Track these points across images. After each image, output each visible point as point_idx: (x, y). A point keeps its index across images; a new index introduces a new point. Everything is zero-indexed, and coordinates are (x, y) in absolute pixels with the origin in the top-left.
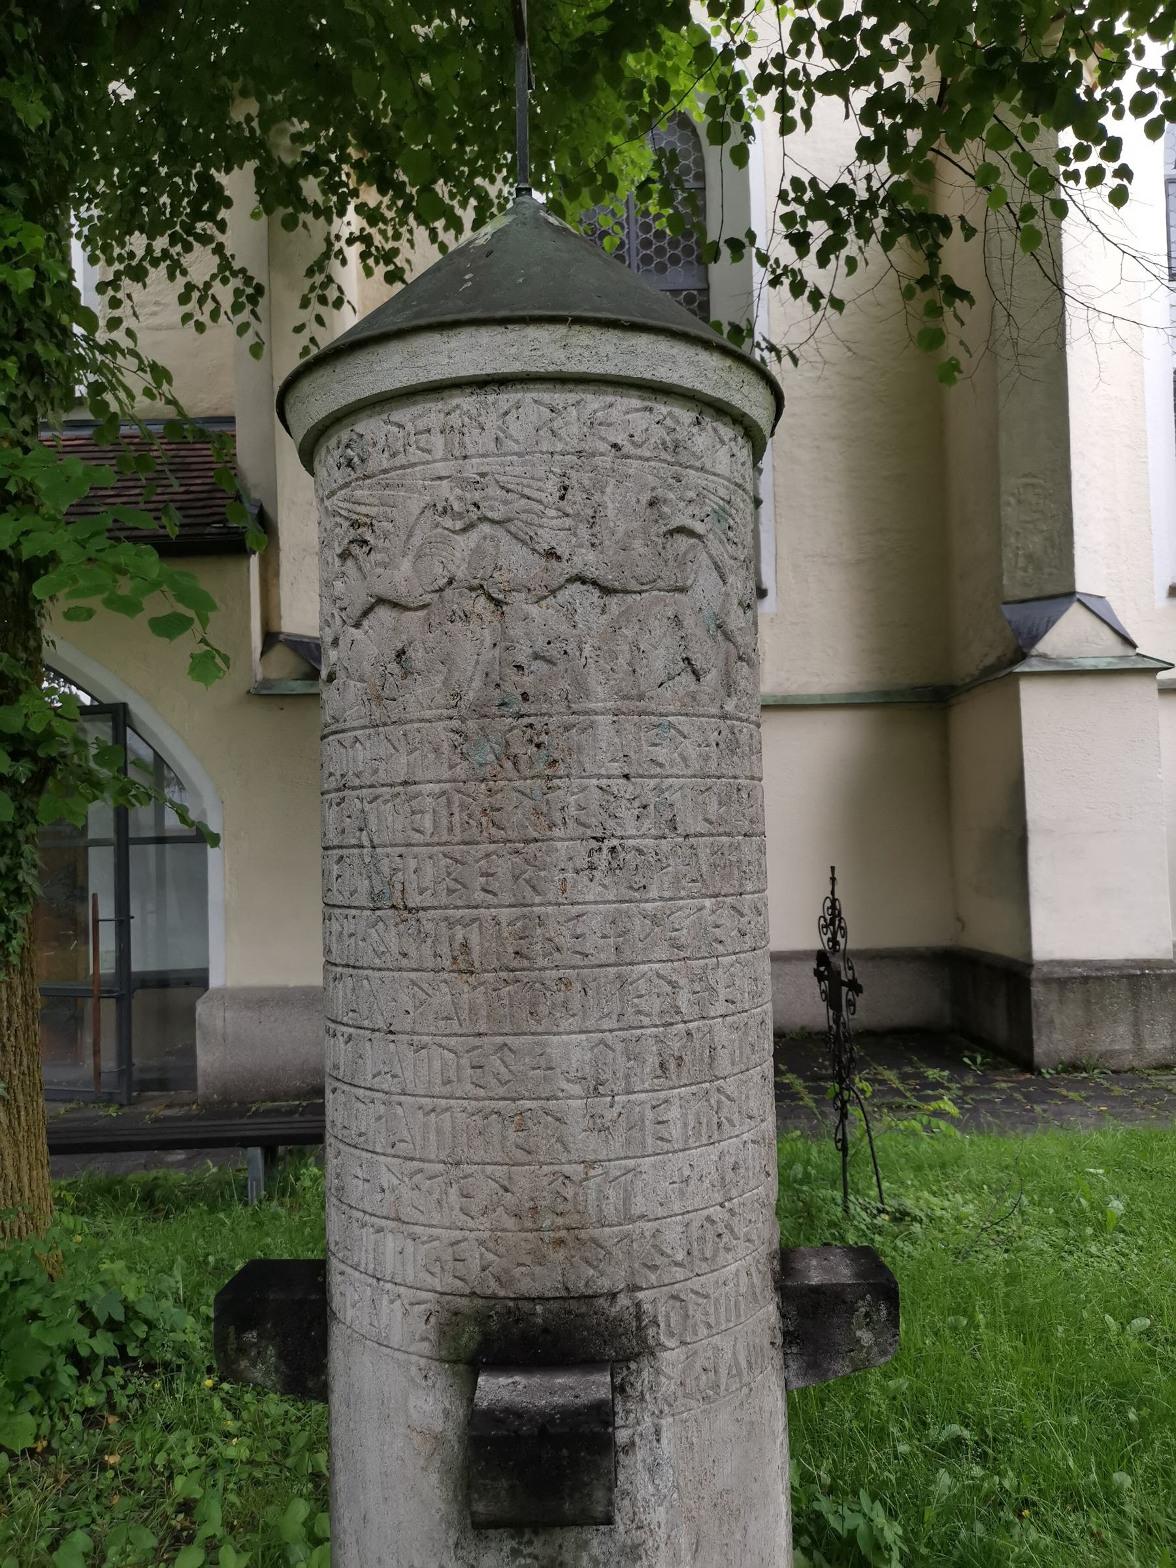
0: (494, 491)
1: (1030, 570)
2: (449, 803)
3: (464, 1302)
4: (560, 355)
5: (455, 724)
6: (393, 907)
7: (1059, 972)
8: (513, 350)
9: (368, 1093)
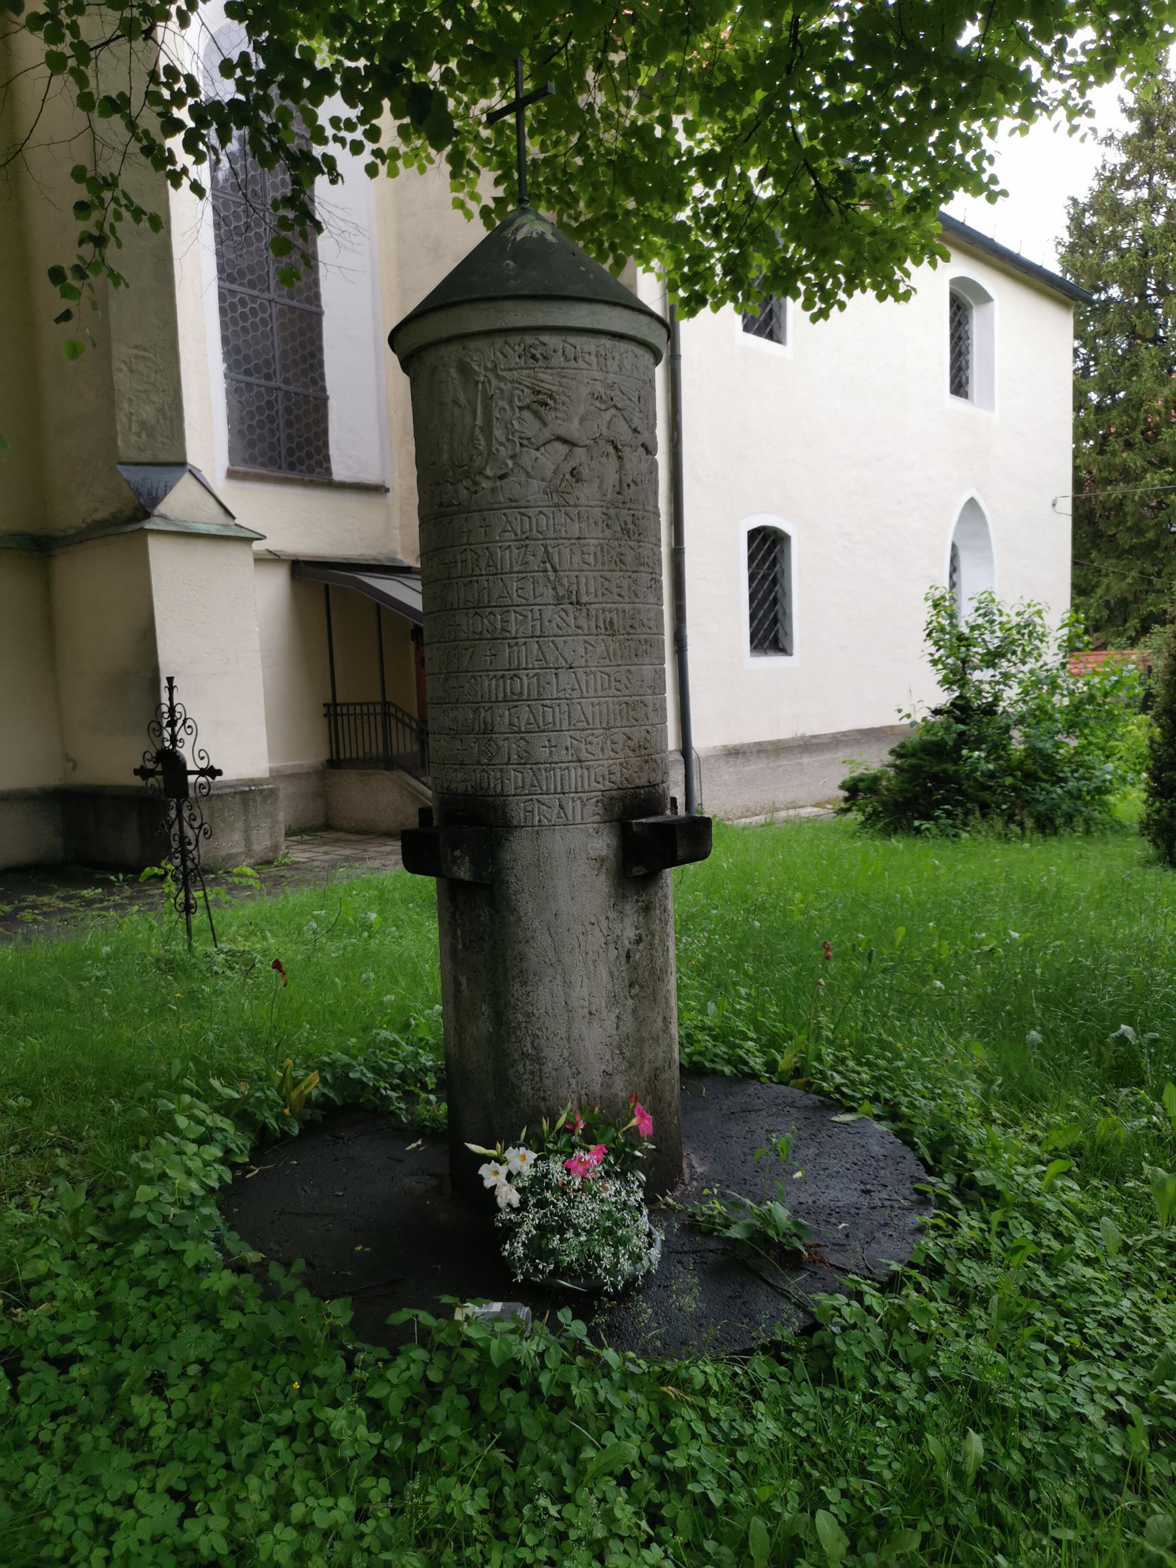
0: (617, 392)
1: (144, 435)
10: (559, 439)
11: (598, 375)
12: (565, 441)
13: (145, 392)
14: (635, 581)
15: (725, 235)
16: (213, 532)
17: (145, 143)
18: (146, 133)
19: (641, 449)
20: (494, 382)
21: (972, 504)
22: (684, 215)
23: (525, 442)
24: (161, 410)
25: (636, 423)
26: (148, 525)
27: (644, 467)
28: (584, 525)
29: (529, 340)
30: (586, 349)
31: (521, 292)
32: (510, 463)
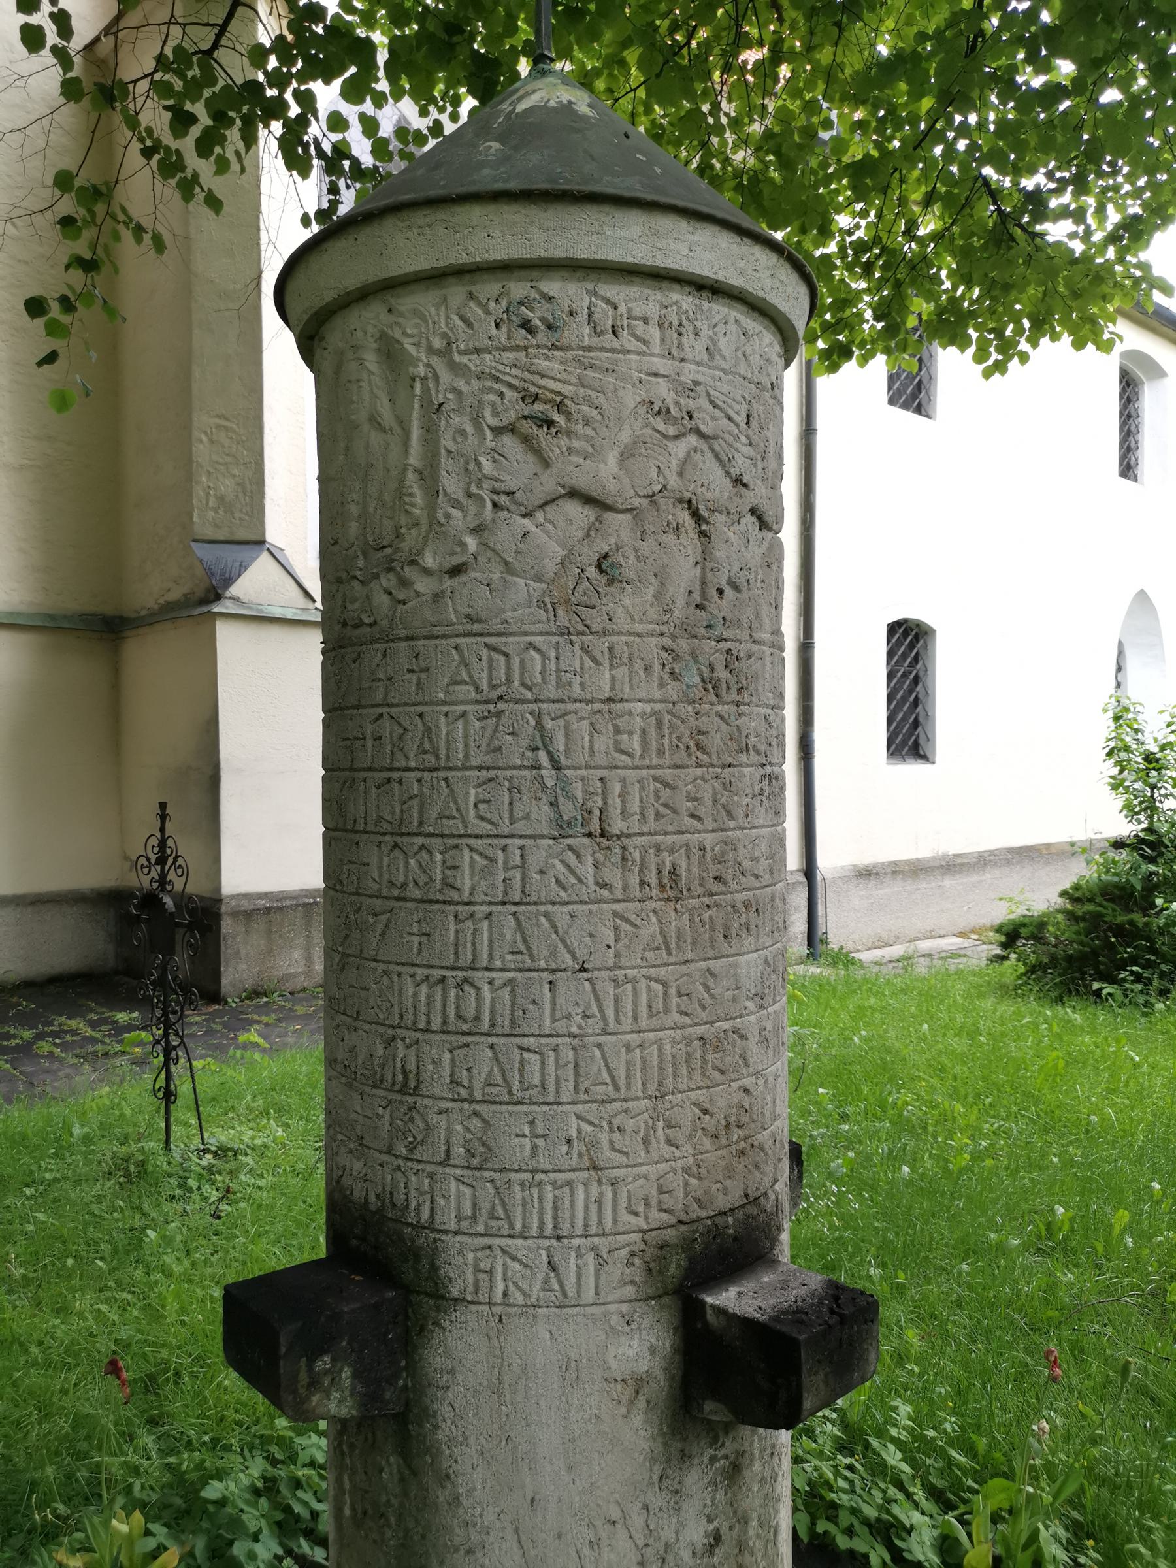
0: (703, 402)
1: (221, 512)
2: (659, 724)
3: (670, 1233)
4: (768, 283)
5: (666, 641)
6: (589, 835)
7: (246, 905)
8: (742, 264)
9: (549, 1040)
10: (573, 494)
11: (663, 365)
12: (588, 500)
13: (226, 464)
14: (728, 786)
15: (877, 275)
16: (289, 616)
17: (149, 143)
18: (149, 131)
19: (750, 520)
20: (445, 377)
22: (832, 248)
23: (503, 500)
24: (241, 484)
25: (741, 465)
26: (217, 608)
27: (754, 555)
28: (622, 672)
29: (518, 289)
30: (638, 309)
31: (499, 186)
32: (472, 543)
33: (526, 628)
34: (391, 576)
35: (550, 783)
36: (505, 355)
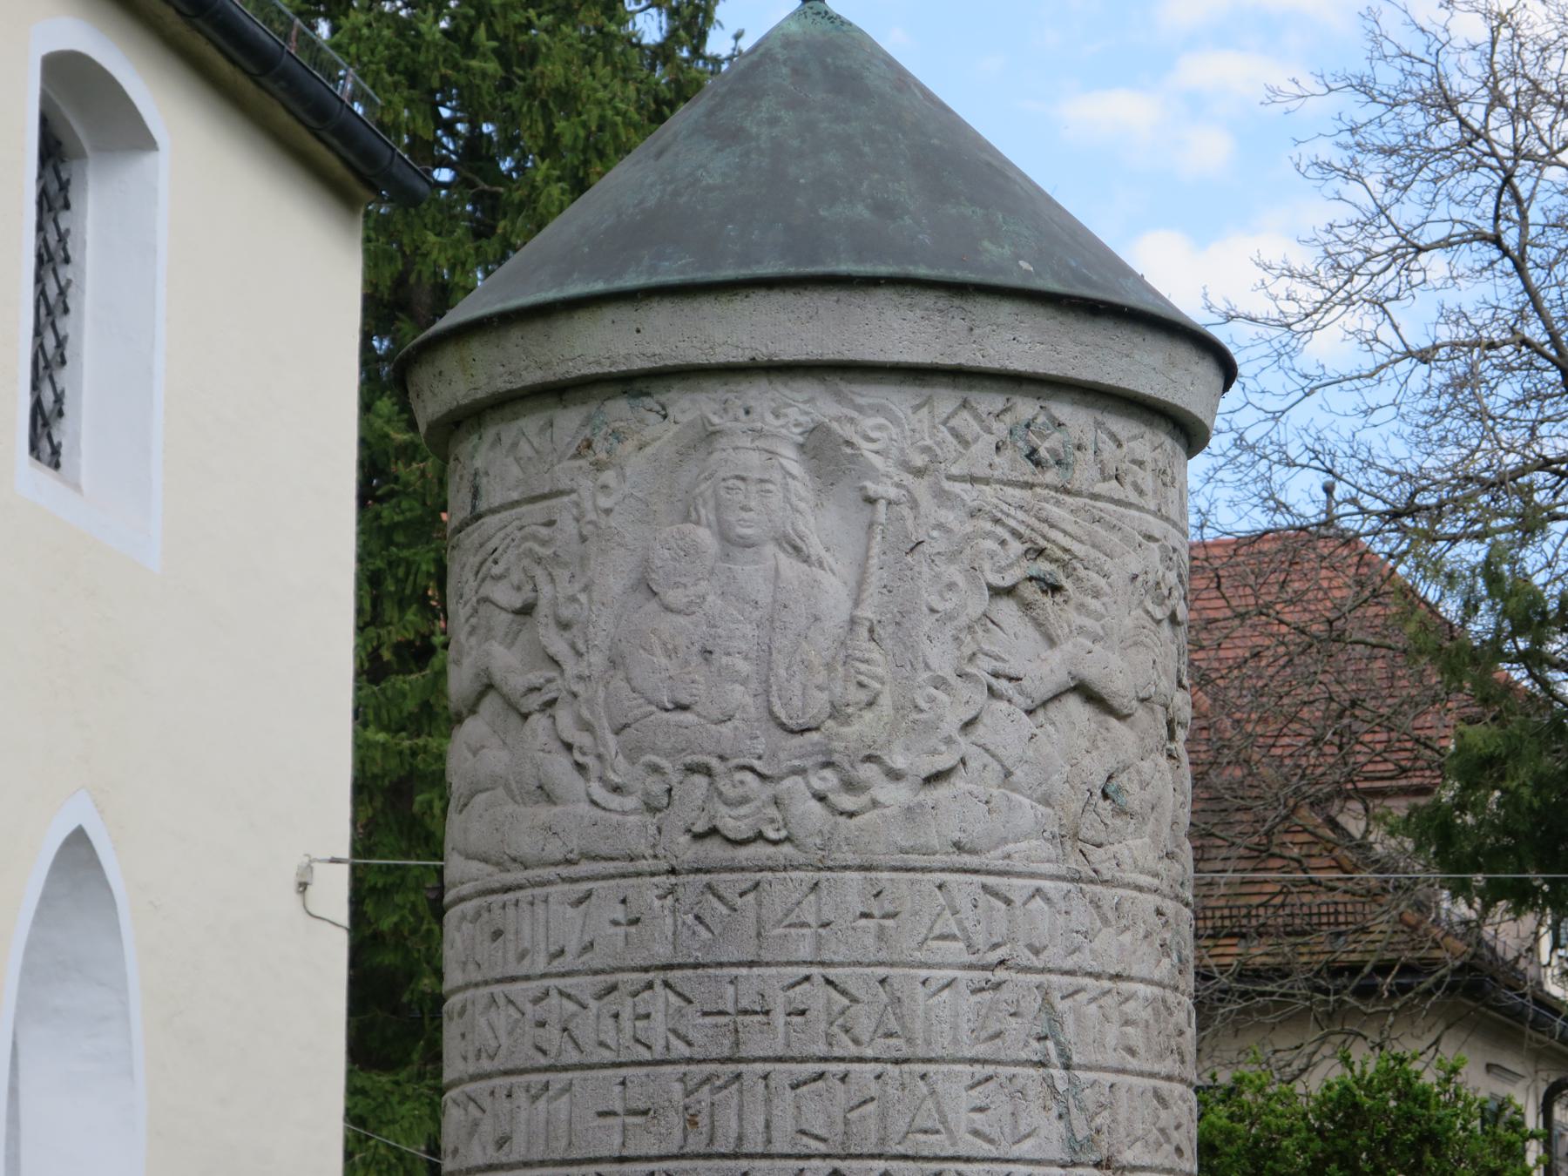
21: (78, 840)
23: (1002, 685)
33: (1034, 867)
34: (828, 773)
35: (1061, 1086)
36: (1009, 490)
